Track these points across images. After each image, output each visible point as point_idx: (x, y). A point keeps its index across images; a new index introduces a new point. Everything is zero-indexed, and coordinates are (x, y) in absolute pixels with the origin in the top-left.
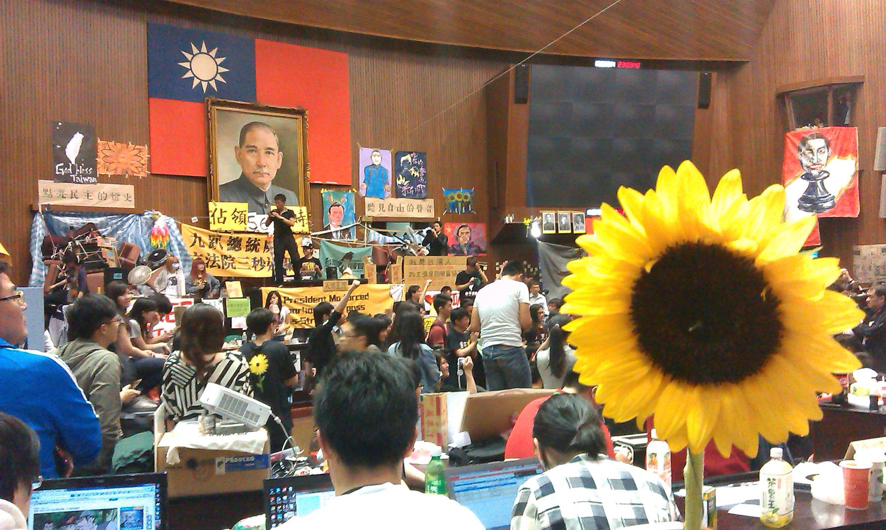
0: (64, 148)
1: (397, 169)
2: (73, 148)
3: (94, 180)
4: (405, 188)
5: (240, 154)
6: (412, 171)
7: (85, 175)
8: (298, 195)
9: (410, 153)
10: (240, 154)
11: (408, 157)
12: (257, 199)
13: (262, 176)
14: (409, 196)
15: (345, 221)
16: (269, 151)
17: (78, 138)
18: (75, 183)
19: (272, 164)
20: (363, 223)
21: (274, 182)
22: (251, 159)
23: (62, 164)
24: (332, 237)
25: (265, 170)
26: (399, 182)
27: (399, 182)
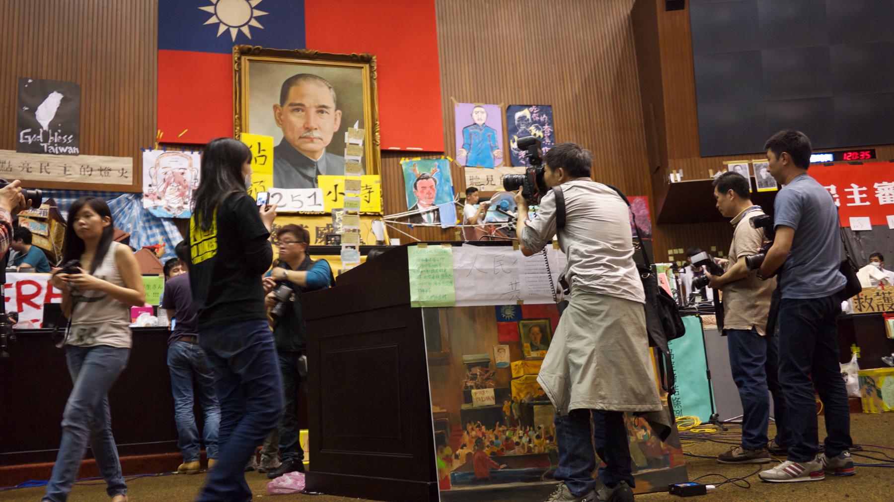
0: (33, 110)
1: (510, 129)
2: (47, 110)
3: (75, 150)
5: (280, 114)
7: (61, 144)
9: (529, 106)
10: (280, 114)
11: (526, 112)
12: (304, 171)
13: (311, 140)
16: (321, 109)
17: (54, 101)
18: (48, 153)
19: (326, 127)
22: (297, 120)
23: (29, 130)
24: (422, 220)
25: (316, 134)
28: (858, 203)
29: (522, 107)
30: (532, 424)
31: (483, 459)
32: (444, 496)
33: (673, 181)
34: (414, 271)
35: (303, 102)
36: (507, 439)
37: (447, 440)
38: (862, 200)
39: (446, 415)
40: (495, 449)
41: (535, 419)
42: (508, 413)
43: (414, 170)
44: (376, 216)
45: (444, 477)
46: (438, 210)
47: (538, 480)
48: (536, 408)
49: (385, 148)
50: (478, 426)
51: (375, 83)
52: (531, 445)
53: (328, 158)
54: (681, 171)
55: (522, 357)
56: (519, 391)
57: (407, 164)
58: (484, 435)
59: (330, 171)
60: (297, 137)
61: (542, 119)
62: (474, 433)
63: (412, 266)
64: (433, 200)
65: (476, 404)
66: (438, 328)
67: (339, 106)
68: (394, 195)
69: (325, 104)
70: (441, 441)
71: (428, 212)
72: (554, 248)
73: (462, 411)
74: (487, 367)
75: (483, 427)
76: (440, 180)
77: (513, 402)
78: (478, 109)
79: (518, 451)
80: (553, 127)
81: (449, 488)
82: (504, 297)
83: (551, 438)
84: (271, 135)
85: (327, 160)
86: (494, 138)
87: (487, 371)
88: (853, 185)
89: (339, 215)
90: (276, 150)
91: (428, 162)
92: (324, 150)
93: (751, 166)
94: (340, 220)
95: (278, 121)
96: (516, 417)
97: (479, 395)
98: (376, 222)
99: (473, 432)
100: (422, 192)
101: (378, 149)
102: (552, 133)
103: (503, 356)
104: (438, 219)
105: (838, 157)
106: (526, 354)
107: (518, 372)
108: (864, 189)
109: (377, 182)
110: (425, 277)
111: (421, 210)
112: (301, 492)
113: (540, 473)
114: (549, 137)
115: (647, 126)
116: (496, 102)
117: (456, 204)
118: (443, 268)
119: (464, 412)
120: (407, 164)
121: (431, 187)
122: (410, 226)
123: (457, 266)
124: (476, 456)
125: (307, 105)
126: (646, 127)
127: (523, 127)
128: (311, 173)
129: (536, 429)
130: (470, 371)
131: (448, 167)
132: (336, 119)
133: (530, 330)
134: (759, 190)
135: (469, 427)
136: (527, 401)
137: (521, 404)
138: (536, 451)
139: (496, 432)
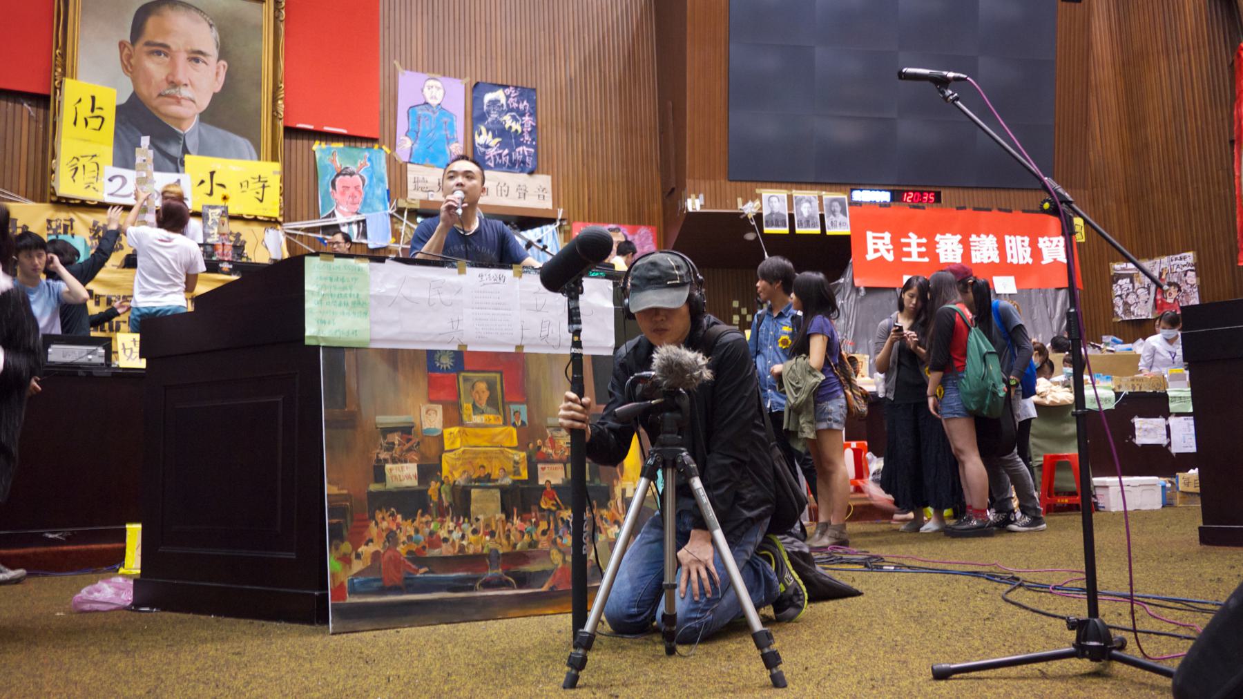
4: (492, 152)
5: (130, 57)
6: (508, 121)
8: (258, 148)
9: (505, 87)
11: (500, 95)
12: (163, 146)
13: (178, 101)
14: (499, 167)
15: (365, 203)
16: (196, 57)
19: (203, 83)
20: (400, 211)
21: (208, 117)
22: (155, 68)
25: (185, 92)
26: (480, 140)
27: (480, 140)
28: (915, 258)
29: (495, 86)
30: (467, 514)
31: (396, 561)
32: (337, 610)
33: (690, 210)
34: (312, 293)
35: (169, 42)
36: (432, 533)
37: (345, 533)
38: (921, 255)
39: (347, 497)
40: (414, 547)
41: (472, 508)
42: (435, 498)
43: (333, 161)
44: (271, 222)
45: (337, 584)
46: (364, 221)
47: (471, 589)
48: (475, 493)
49: (291, 124)
50: (392, 515)
51: (282, 27)
52: (465, 543)
53: (203, 131)
54: (701, 196)
55: (460, 423)
56: (453, 468)
57: (322, 150)
58: (398, 527)
59: (204, 150)
60: (155, 95)
61: (521, 107)
62: (384, 525)
63: (310, 285)
64: (359, 207)
65: (391, 484)
66: (343, 376)
67: (223, 54)
68: (299, 194)
69: (203, 49)
70: (337, 535)
71: (349, 224)
72: (515, 275)
73: (371, 494)
74: (410, 433)
75: (399, 517)
76: (371, 178)
77: (442, 483)
78: (431, 83)
79: (445, 550)
80: (536, 120)
81: (344, 598)
82: (439, 338)
83: (492, 534)
84: (114, 87)
85: (200, 134)
86: (452, 124)
87: (409, 440)
88: (911, 234)
89: (214, 215)
90: (119, 109)
91: (354, 152)
92: (196, 118)
93: (790, 198)
94: (214, 222)
95: (125, 67)
96: (446, 504)
97: (394, 472)
98: (271, 231)
99: (384, 522)
100: (343, 194)
101: (281, 124)
102: (534, 128)
103: (432, 419)
104: (364, 234)
105: (896, 196)
106: (465, 418)
107: (453, 443)
108: (924, 240)
109: (275, 173)
110: (328, 303)
111: (340, 219)
112: (126, 608)
113: (475, 580)
114: (530, 133)
115: (663, 132)
116: (458, 75)
117: (392, 216)
118: (354, 292)
119: (373, 496)
120: (322, 150)
121: (356, 188)
122: (322, 240)
123: (376, 289)
124: (386, 556)
125: (173, 47)
126: (661, 133)
127: (494, 115)
128: (174, 150)
129: (473, 520)
130: (385, 438)
131: (384, 161)
132: (217, 74)
133: (473, 387)
134: (799, 231)
135: (379, 516)
136: (462, 483)
137: (454, 487)
138: (471, 551)
139: (416, 524)
